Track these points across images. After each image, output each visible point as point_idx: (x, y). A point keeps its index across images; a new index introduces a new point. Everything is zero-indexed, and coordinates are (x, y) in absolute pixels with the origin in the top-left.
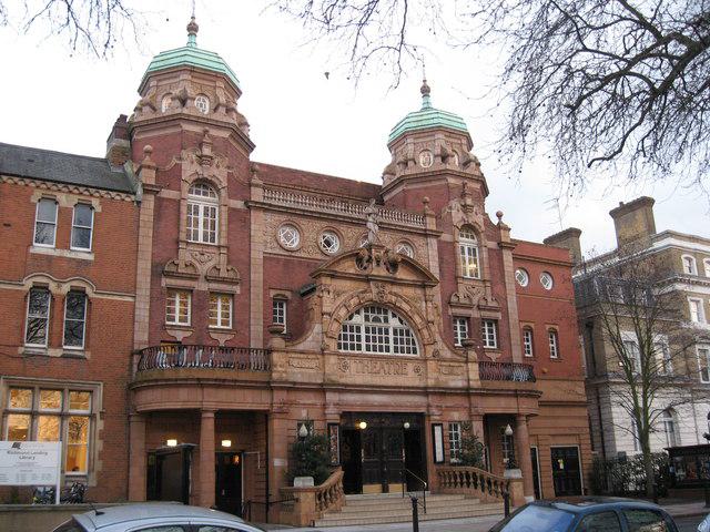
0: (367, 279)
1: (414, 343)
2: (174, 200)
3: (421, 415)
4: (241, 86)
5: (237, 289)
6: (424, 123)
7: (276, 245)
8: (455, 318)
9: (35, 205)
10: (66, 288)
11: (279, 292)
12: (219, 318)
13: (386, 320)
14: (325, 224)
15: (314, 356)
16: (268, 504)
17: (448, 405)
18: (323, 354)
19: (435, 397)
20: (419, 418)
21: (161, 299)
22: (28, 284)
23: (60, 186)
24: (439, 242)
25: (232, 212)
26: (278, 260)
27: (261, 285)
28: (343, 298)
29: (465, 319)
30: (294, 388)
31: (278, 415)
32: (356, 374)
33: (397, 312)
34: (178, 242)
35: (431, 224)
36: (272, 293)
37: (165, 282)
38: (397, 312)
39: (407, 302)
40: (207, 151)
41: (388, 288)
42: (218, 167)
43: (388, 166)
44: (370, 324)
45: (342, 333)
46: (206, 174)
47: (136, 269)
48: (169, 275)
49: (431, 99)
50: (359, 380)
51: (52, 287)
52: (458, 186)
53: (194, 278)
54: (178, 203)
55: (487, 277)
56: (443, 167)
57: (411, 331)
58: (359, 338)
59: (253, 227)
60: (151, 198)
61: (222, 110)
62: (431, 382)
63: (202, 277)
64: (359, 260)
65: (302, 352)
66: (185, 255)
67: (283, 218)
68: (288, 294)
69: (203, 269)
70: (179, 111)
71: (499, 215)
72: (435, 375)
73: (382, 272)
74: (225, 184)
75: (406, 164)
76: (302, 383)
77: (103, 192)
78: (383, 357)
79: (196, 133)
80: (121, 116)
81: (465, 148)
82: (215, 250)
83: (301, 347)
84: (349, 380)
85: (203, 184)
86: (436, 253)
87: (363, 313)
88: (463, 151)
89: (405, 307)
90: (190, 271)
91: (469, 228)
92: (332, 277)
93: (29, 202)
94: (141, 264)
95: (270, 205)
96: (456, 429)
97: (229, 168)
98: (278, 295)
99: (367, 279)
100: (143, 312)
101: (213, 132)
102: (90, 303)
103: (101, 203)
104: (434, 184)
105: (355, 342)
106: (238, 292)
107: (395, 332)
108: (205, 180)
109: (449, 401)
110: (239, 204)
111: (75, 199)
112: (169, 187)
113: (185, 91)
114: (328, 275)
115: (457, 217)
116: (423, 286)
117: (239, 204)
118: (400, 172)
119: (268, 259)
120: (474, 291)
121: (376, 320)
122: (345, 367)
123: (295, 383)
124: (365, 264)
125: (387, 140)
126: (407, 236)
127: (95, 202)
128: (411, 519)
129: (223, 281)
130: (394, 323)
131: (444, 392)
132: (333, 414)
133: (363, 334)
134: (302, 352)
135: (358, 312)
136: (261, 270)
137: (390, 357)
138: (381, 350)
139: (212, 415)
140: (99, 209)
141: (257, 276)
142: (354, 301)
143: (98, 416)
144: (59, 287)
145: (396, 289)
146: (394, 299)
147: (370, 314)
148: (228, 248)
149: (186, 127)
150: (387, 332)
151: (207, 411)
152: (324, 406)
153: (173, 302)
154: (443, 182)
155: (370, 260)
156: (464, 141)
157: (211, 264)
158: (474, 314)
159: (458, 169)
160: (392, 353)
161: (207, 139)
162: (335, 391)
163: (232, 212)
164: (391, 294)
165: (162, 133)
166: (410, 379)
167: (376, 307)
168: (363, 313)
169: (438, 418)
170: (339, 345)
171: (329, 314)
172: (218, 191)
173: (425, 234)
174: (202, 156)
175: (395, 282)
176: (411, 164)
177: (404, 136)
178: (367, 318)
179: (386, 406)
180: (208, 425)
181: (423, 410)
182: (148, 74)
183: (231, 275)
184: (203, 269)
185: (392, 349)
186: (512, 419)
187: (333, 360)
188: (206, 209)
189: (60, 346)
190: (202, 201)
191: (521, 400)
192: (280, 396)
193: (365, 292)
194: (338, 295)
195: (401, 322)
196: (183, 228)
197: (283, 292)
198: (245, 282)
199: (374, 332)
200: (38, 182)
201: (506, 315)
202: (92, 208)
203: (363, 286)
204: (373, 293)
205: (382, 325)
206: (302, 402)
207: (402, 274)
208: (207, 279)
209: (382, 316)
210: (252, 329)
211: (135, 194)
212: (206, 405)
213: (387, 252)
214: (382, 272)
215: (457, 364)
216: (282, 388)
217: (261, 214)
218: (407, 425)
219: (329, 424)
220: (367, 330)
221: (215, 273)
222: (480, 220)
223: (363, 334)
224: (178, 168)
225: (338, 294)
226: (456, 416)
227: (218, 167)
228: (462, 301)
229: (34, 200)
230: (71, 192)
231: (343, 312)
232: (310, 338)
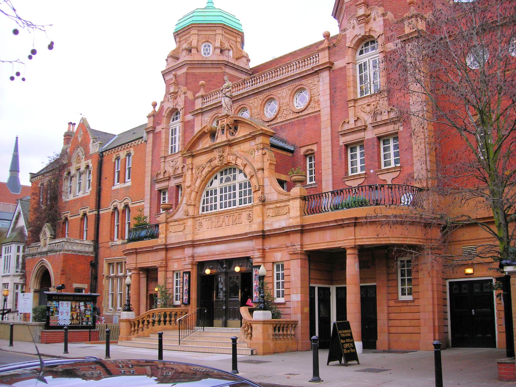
13: (234, 178)
17: (273, 246)
29: (361, 143)
44: (224, 184)
45: (206, 198)
78: (233, 210)
86: (327, 87)
87: (219, 177)
92: (193, 156)
107: (241, 185)
121: (228, 180)
128: (231, 352)
131: (264, 236)
134: (175, 221)
135: (216, 178)
137: (237, 210)
206: (175, 257)
218: (237, 269)
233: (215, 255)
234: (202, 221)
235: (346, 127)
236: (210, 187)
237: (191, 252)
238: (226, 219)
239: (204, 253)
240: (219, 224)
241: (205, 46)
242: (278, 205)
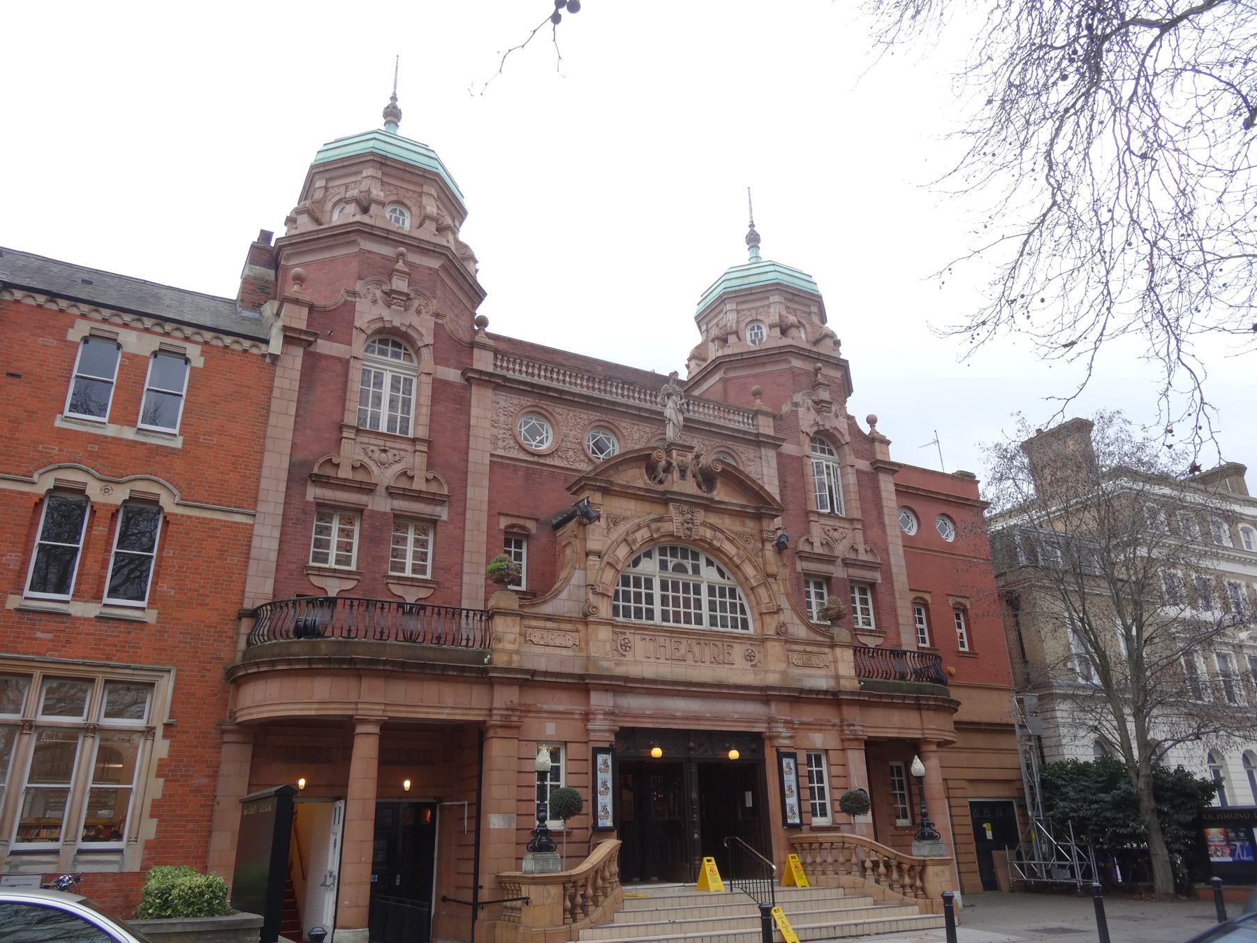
0: (665, 499)
1: (743, 611)
2: (340, 359)
3: (758, 738)
4: (467, 203)
5: (443, 513)
6: (746, 281)
7: (512, 443)
8: (808, 576)
9: (75, 346)
10: (119, 495)
11: (515, 521)
12: (409, 561)
13: (696, 570)
14: (595, 415)
15: (569, 626)
16: (476, 905)
17: (805, 719)
18: (586, 624)
19: (781, 706)
20: (753, 742)
21: (304, 519)
22: (44, 483)
23: (127, 318)
24: (779, 455)
25: (440, 387)
26: (516, 469)
27: (485, 507)
28: (622, 529)
29: (824, 581)
30: (530, 680)
31: (501, 732)
32: (644, 660)
33: (715, 555)
34: (341, 427)
35: (766, 427)
36: (504, 522)
37: (313, 493)
38: (715, 555)
39: (731, 541)
40: (400, 284)
41: (700, 516)
42: (418, 312)
43: (698, 347)
44: (670, 575)
45: (621, 588)
46: (395, 317)
47: (260, 467)
48: (320, 480)
49: (762, 253)
50: (649, 670)
51: (94, 491)
52: (806, 372)
53: (368, 489)
54: (345, 363)
55: (857, 514)
56: (786, 341)
57: (739, 591)
58: (650, 599)
59: (474, 411)
60: (299, 352)
61: (431, 226)
62: (772, 679)
63: (381, 490)
64: (651, 469)
65: (549, 618)
66: (351, 452)
67: (527, 401)
68: (531, 526)
69: (385, 477)
70: (358, 218)
71: (872, 421)
72: (782, 666)
73: (690, 487)
74: (429, 339)
75: (724, 340)
76: (546, 673)
77: (208, 336)
79: (384, 257)
80: (263, 232)
81: (816, 320)
82: (409, 447)
83: (547, 609)
84: (633, 670)
85: (393, 339)
88: (812, 324)
89: (729, 548)
90: (360, 476)
91: (825, 439)
92: (606, 492)
93: (62, 338)
94: (269, 460)
95: (505, 378)
96: (819, 764)
97: (437, 315)
98: (513, 526)
99: (665, 499)
100: (266, 541)
101: (414, 258)
102: (166, 523)
103: (203, 353)
104: (769, 368)
105: (644, 605)
106: (445, 517)
107: (711, 590)
108: (395, 331)
109: (809, 714)
110: (453, 375)
111: (154, 343)
112: (329, 338)
113: (369, 191)
114: (599, 489)
115: (807, 420)
116: (758, 517)
117: (453, 375)
118: (714, 352)
119: (498, 464)
120: (836, 535)
121: (679, 568)
122: (626, 647)
123: (534, 673)
124: (662, 475)
125: (694, 310)
126: (729, 443)
127: (193, 351)
129: (417, 496)
130: (709, 575)
132: (602, 730)
133: (657, 592)
134: (549, 618)
135: (648, 555)
136: (486, 482)
137: (702, 634)
138: (688, 621)
139: (375, 729)
140: (198, 362)
141: (478, 493)
142: (643, 534)
143: (159, 732)
144: (106, 491)
145: (713, 519)
146: (709, 534)
147: (669, 558)
148: (429, 442)
149: (367, 245)
150: (697, 590)
151: (364, 721)
152: (587, 717)
153: (327, 530)
154: (784, 366)
155: (668, 469)
156: (814, 309)
157: (398, 468)
158: (838, 572)
159: (808, 347)
160: (706, 624)
161: (400, 265)
162: (607, 689)
163: (440, 387)
164: (705, 526)
165: (327, 255)
166: (738, 672)
167: (678, 548)
168: (657, 557)
169: (787, 742)
170: (616, 610)
171: (599, 555)
172: (417, 351)
173: (757, 442)
174: (393, 291)
175: (710, 506)
176: (732, 339)
177: (722, 299)
178: (663, 566)
179: (697, 718)
180: (365, 751)
181: (760, 728)
182: (312, 167)
183: (433, 488)
184: (385, 477)
185: (706, 619)
186: (914, 747)
187: (604, 633)
188: (395, 380)
189: (97, 597)
190: (389, 367)
191: (925, 713)
192: (505, 697)
193: (660, 520)
194: (615, 524)
195: (722, 574)
196: (353, 404)
197: (521, 522)
198: (456, 499)
199: (675, 589)
200: (85, 308)
201: (888, 577)
202: (187, 361)
203: (657, 511)
204: (675, 522)
205: (689, 577)
206: (546, 707)
207: (720, 494)
208: (391, 493)
209: (688, 564)
210: (466, 579)
211: (267, 342)
212: (363, 711)
213: (697, 457)
214: (690, 487)
215: (815, 649)
216: (510, 682)
217: (489, 393)
219: (597, 751)
220: (664, 586)
221: (403, 483)
222: (843, 425)
223: (657, 592)
224: (349, 308)
225: (615, 521)
226: (818, 740)
227: (418, 312)
228: (818, 549)
229: (74, 335)
230: (147, 330)
231: (622, 552)
232: (564, 595)
233: (675, 718)
234: (631, 637)
235: (807, 548)
236: (632, 569)
237: (611, 703)
238: (696, 649)
239: (643, 709)
240: (678, 655)
241: (753, 329)
242: (809, 649)
